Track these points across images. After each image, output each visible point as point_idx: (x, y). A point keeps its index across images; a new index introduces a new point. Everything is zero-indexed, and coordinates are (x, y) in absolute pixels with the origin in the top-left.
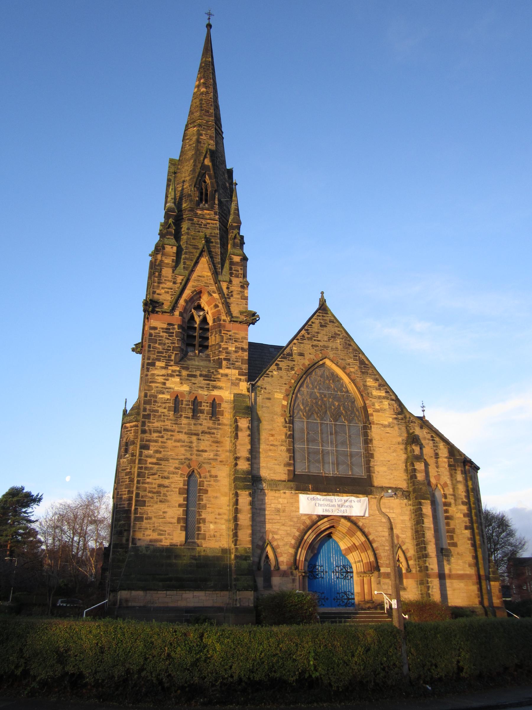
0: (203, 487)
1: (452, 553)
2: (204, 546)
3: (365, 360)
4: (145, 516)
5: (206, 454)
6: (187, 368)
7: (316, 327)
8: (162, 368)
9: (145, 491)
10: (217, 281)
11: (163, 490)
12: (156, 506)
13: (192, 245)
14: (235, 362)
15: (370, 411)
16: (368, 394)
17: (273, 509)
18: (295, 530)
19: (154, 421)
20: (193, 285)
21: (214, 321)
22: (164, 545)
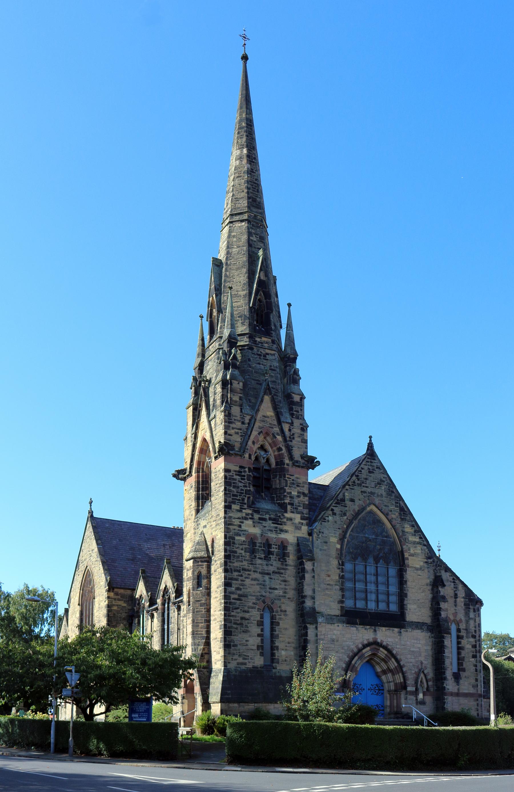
0: (276, 620)
1: (461, 676)
2: (278, 668)
3: (404, 507)
4: (232, 644)
5: (276, 591)
6: (257, 511)
7: (365, 472)
8: (238, 511)
9: (231, 622)
10: (280, 422)
11: (245, 622)
12: (240, 635)
13: (255, 380)
14: (298, 506)
15: (406, 555)
16: (406, 539)
17: (330, 639)
18: (346, 657)
19: (234, 561)
20: (259, 426)
21: (277, 464)
22: (248, 668)
